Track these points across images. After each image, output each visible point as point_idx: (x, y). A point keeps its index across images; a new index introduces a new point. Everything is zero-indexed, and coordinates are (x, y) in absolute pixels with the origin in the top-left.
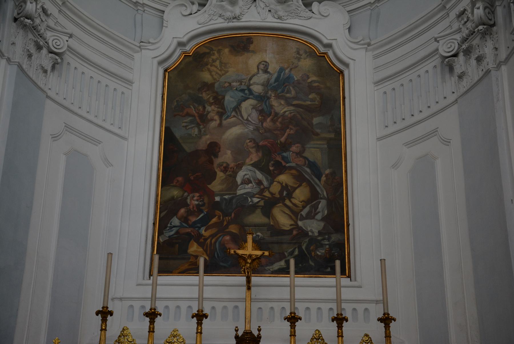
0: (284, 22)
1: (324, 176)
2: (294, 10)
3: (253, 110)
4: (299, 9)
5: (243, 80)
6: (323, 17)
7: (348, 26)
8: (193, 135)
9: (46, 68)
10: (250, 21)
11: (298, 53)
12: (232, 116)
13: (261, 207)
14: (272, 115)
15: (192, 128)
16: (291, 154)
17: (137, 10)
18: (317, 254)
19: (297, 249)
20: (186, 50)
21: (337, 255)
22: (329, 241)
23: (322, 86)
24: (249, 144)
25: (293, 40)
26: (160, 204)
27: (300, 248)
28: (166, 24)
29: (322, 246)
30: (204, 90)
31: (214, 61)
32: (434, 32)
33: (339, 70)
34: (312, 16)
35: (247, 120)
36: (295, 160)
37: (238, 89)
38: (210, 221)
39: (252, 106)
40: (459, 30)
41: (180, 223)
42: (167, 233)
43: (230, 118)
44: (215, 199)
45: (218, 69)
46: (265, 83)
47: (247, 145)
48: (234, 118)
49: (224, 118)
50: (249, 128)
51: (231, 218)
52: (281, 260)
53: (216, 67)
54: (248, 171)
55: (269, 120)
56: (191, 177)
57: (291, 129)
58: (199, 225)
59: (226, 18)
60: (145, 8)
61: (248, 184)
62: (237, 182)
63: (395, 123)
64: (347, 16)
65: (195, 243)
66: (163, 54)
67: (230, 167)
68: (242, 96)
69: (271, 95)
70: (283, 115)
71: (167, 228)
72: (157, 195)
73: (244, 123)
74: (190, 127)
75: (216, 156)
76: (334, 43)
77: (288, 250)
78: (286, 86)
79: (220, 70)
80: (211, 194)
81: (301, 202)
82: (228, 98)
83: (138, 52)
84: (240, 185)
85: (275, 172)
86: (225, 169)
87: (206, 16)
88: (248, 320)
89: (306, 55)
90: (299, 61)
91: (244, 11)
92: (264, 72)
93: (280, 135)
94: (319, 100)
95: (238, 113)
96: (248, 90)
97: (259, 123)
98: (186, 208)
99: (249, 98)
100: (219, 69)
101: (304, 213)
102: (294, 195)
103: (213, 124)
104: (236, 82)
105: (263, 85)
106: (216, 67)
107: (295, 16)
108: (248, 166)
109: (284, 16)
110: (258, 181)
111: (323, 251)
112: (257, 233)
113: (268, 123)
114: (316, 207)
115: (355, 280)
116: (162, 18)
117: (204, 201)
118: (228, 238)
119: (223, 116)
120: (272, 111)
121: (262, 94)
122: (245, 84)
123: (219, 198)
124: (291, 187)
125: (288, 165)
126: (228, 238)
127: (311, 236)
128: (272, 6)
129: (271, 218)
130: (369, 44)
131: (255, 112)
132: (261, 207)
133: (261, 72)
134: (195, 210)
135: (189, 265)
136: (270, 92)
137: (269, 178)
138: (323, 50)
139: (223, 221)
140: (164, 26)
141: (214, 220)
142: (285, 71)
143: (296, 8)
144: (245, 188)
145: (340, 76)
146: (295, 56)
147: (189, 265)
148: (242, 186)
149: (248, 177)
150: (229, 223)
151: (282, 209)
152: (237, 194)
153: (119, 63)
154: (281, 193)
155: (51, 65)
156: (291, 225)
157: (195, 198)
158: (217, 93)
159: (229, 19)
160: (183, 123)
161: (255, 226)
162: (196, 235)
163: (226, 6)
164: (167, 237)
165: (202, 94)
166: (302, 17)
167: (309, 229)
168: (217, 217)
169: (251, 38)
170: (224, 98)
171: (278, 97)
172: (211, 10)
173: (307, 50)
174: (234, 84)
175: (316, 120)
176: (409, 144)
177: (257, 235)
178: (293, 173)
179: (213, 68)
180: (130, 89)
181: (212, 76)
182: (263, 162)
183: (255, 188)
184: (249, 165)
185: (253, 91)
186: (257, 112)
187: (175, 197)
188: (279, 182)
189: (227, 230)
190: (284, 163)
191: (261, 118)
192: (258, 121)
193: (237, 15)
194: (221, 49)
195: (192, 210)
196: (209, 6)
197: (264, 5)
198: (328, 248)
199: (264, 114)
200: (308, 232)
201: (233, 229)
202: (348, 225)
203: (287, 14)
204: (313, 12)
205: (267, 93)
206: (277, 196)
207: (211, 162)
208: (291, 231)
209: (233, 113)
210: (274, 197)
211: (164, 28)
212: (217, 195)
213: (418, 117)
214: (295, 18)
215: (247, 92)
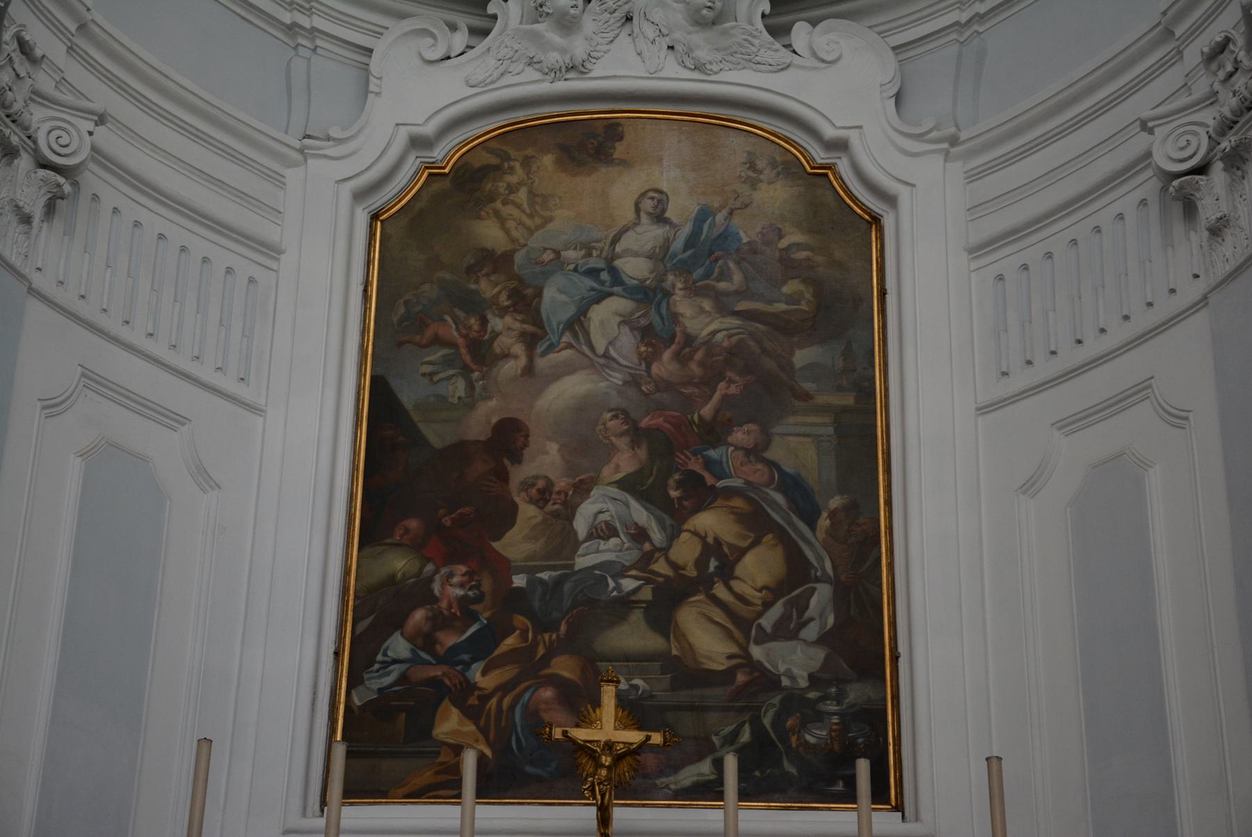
0: (713, 78)
1: (825, 515)
2: (739, 44)
3: (622, 327)
4: (756, 42)
5: (594, 244)
6: (823, 65)
7: (894, 91)
8: (450, 400)
9: (27, 210)
10: (615, 77)
11: (752, 166)
12: (562, 345)
13: (644, 605)
14: (677, 340)
15: (449, 378)
16: (729, 453)
17: (295, 48)
18: (807, 742)
19: (747, 728)
20: (435, 158)
21: (862, 746)
22: (839, 704)
23: (819, 259)
24: (610, 424)
25: (737, 129)
26: (356, 597)
27: (756, 723)
28: (377, 86)
29: (819, 717)
30: (483, 272)
31: (512, 189)
32: (1141, 105)
33: (869, 214)
34: (792, 62)
35: (606, 355)
36: (744, 468)
37: (581, 268)
38: (497, 645)
39: (621, 315)
40: (1212, 98)
41: (412, 650)
42: (373, 681)
43: (558, 349)
44: (512, 582)
45: (523, 211)
46: (657, 250)
47: (606, 429)
48: (569, 352)
49: (539, 350)
50: (612, 379)
51: (558, 636)
52: (700, 758)
53: (519, 206)
54: (608, 501)
55: (667, 355)
56: (443, 520)
57: (731, 381)
58: (466, 657)
59: (547, 68)
60: (319, 42)
61: (606, 538)
62: (575, 533)
63: (1029, 363)
64: (891, 60)
65: (455, 711)
66: (367, 169)
67: (557, 489)
68: (593, 289)
69: (674, 286)
70: (708, 343)
71: (373, 666)
72: (346, 572)
73: (595, 363)
74: (442, 375)
75: (517, 459)
76: (854, 137)
77: (721, 728)
78: (716, 260)
79: (531, 216)
80: (503, 567)
81: (760, 590)
83: (295, 164)
84: (584, 542)
85: (686, 503)
86: (543, 496)
87: (492, 62)
89: (775, 171)
90: (755, 189)
91: (599, 48)
92: (655, 219)
93: (698, 399)
94: (812, 299)
95: (580, 334)
96: (609, 272)
97: (641, 364)
98: (428, 607)
99: (611, 294)
100: (528, 211)
101: (767, 621)
102: (739, 570)
103: (510, 368)
104: (575, 249)
106: (519, 206)
107: (742, 61)
108: (609, 488)
109: (711, 63)
110: (635, 529)
111: (821, 731)
112: (632, 679)
113: (665, 366)
114: (801, 605)
115: (917, 819)
116: (367, 70)
117: (482, 589)
118: (547, 693)
119: (538, 347)
120: (678, 329)
121: (648, 282)
122: (601, 252)
123: (525, 580)
124: (730, 545)
125: (721, 484)
126: (547, 693)
127: (786, 688)
128: (678, 35)
129: (672, 635)
130: (954, 141)
131: (629, 333)
132: (644, 605)
133: (644, 219)
134: (454, 614)
135: (437, 773)
136: (671, 278)
137: (668, 521)
138: (823, 159)
139: (535, 644)
140: (372, 92)
141: (510, 642)
142: (714, 217)
143: (745, 40)
144: (598, 551)
145: (871, 232)
146: (743, 174)
147: (437, 773)
148: (590, 545)
149: (609, 518)
150: (551, 653)
151: (704, 611)
152: (576, 568)
153: (241, 196)
154: (701, 563)
155: (42, 201)
156: (730, 657)
157: (456, 580)
158: (520, 280)
159: (555, 72)
160: (422, 364)
161: (628, 661)
162: (459, 687)
163: (546, 34)
164: (373, 690)
165: (477, 282)
166: (764, 64)
167: (782, 668)
168: (518, 632)
169: (618, 125)
170: (539, 294)
171: (694, 291)
172: (503, 45)
173: (778, 159)
174: (570, 254)
175: (802, 357)
176: (1071, 424)
177: (631, 686)
178: (736, 507)
179: (508, 210)
180: (272, 270)
181: (507, 232)
182: (651, 475)
183: (627, 549)
184: (609, 484)
185: (623, 275)
186: (636, 333)
187: (399, 575)
188: (695, 533)
189: (547, 671)
190: (709, 480)
191: (645, 351)
192: (636, 361)
193: (578, 61)
194: (533, 157)
195: (445, 611)
196: (500, 35)
197: (655, 31)
198: (835, 724)
200: (779, 676)
201: (564, 666)
202: (895, 658)
203: (719, 56)
204: (794, 52)
205: (661, 279)
206: (692, 572)
207: (503, 477)
208: (729, 674)
209: (567, 338)
210: (682, 575)
211: (371, 96)
212: (520, 570)
213: (1094, 347)
214: (744, 68)
215: (605, 276)
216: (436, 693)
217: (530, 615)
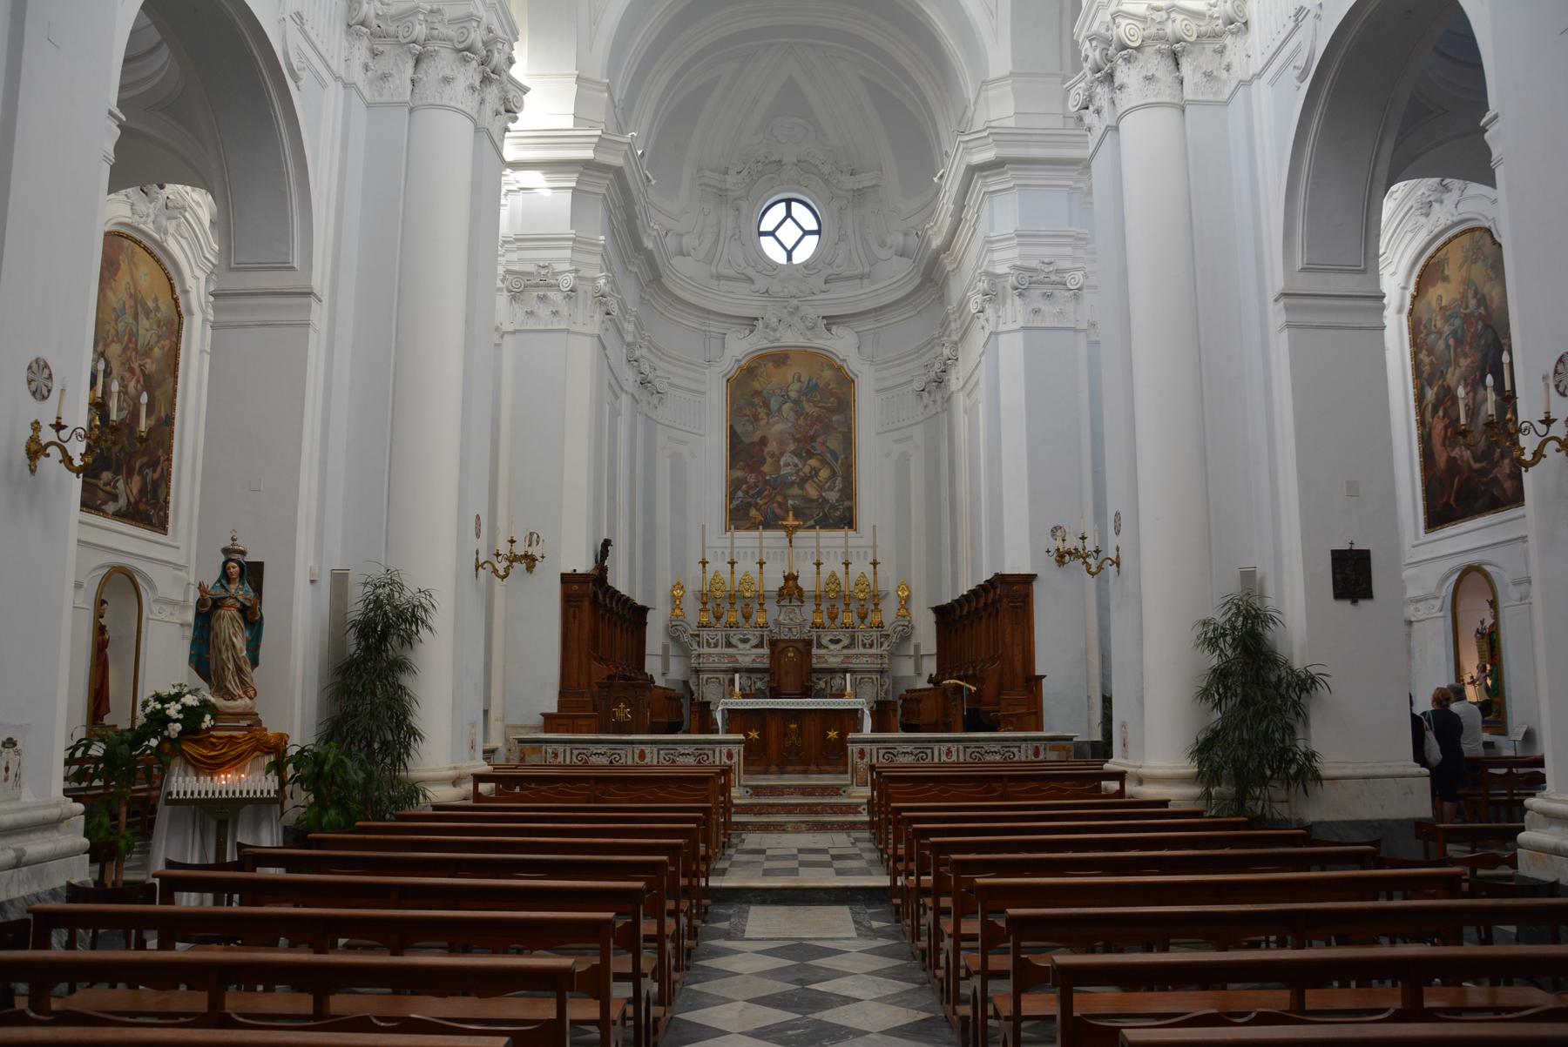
27: (824, 511)
52: (811, 519)
55: (802, 418)
75: (766, 446)
76: (847, 358)
80: (763, 474)
82: (772, 402)
86: (772, 456)
88: (790, 567)
101: (826, 487)
103: (763, 422)
105: (797, 391)
113: (801, 421)
118: (775, 505)
126: (775, 505)
141: (766, 493)
154: (810, 473)
159: (772, 342)
170: (769, 403)
171: (808, 401)
175: (834, 419)
176: (897, 441)
179: (761, 379)
188: (809, 465)
199: (798, 414)
207: (763, 451)
208: (817, 500)
216: (749, 505)
217: (771, 486)
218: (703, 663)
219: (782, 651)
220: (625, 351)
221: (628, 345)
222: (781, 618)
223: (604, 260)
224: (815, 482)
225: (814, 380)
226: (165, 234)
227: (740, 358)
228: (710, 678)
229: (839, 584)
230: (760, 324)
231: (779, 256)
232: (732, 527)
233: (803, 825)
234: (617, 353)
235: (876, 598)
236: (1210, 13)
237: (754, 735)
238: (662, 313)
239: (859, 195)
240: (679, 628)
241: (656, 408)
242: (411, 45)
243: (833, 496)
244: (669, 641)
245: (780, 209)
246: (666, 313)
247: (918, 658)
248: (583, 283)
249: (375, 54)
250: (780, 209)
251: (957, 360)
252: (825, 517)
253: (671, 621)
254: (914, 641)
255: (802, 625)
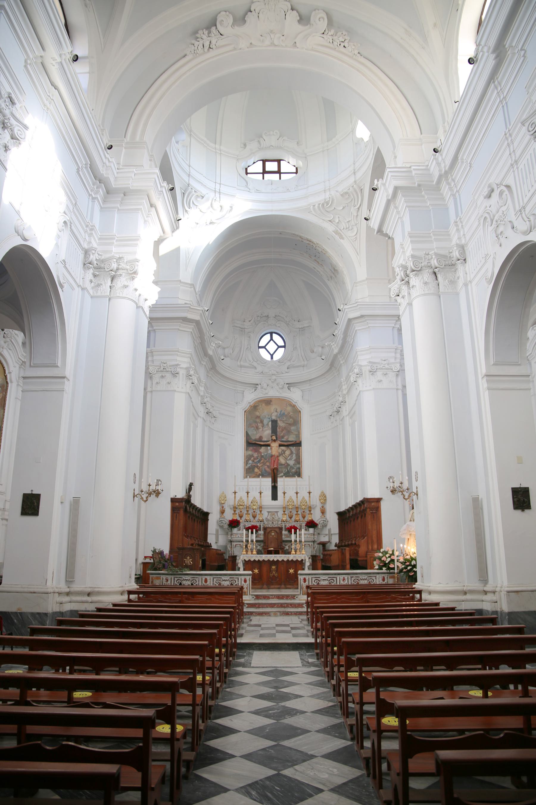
27: (287, 469)
29: (294, 468)
49: (264, 427)
52: (282, 473)
72: (245, 454)
80: (261, 453)
82: (264, 421)
101: (289, 458)
102: (286, 453)
103: (261, 430)
105: (276, 416)
114: (292, 456)
118: (266, 466)
126: (266, 466)
141: (262, 461)
154: (282, 452)
171: (280, 420)
175: (293, 428)
206: (281, 453)
208: (285, 464)
209: (267, 426)
218: (234, 538)
219: (269, 533)
220: (200, 399)
221: (201, 396)
222: (269, 517)
223: (191, 360)
224: (284, 456)
225: (283, 411)
226: (2, 348)
227: (250, 402)
228: (237, 545)
229: (293, 502)
230: (259, 387)
231: (267, 357)
232: (248, 477)
233: (278, 613)
234: (197, 400)
235: (310, 509)
236: (449, 255)
237: (256, 571)
238: (216, 382)
239: (303, 329)
240: (223, 522)
241: (213, 424)
242: (110, 272)
243: (291, 463)
244: (218, 528)
245: (268, 337)
246: (217, 382)
247: (330, 535)
248: (181, 370)
249: (95, 276)
250: (267, 337)
251: (345, 402)
252: (288, 472)
253: (219, 519)
254: (328, 527)
255: (278, 521)
